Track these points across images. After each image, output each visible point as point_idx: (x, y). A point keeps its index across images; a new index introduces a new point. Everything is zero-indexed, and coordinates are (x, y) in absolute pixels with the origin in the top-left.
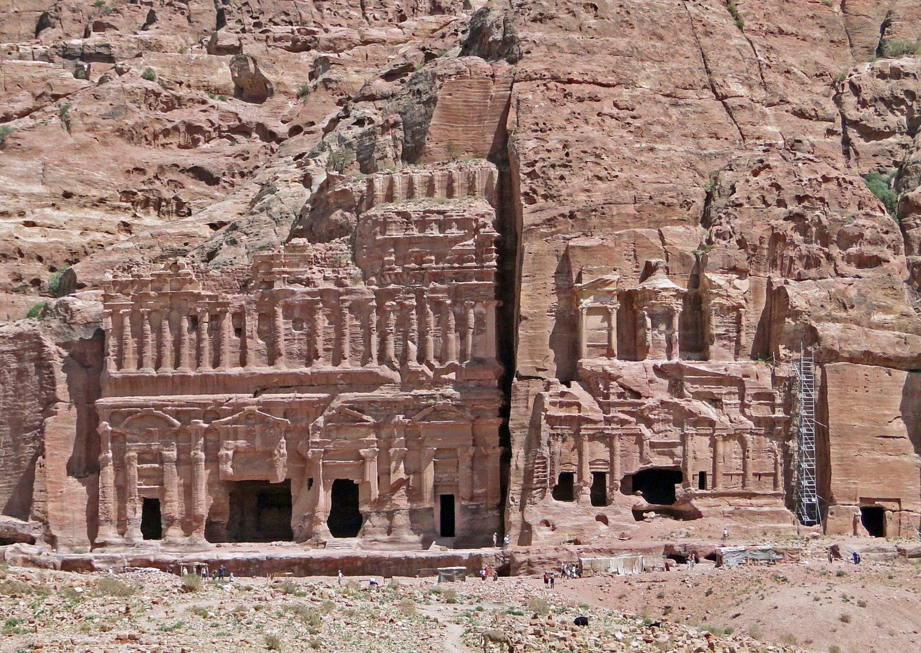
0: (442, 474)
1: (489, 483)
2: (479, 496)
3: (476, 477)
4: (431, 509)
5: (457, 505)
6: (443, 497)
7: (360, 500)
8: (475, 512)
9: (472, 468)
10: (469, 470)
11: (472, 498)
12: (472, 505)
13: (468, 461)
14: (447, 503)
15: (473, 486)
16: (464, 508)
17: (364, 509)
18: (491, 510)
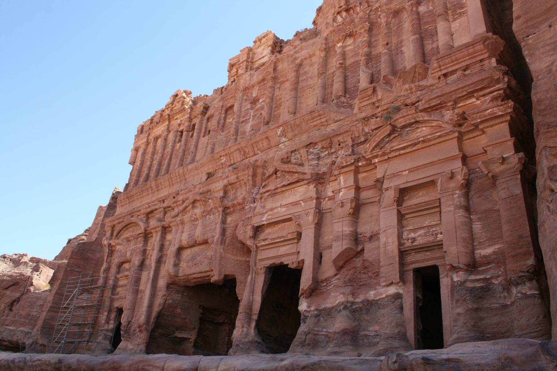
0: (415, 230)
1: (505, 228)
2: (487, 261)
3: (477, 226)
4: (398, 296)
5: (445, 283)
6: (417, 271)
7: (300, 293)
8: (483, 293)
9: (467, 209)
10: (461, 212)
11: (473, 266)
12: (475, 280)
13: (458, 197)
14: (427, 282)
15: (471, 241)
16: (454, 287)
17: (303, 306)
18: (517, 284)
